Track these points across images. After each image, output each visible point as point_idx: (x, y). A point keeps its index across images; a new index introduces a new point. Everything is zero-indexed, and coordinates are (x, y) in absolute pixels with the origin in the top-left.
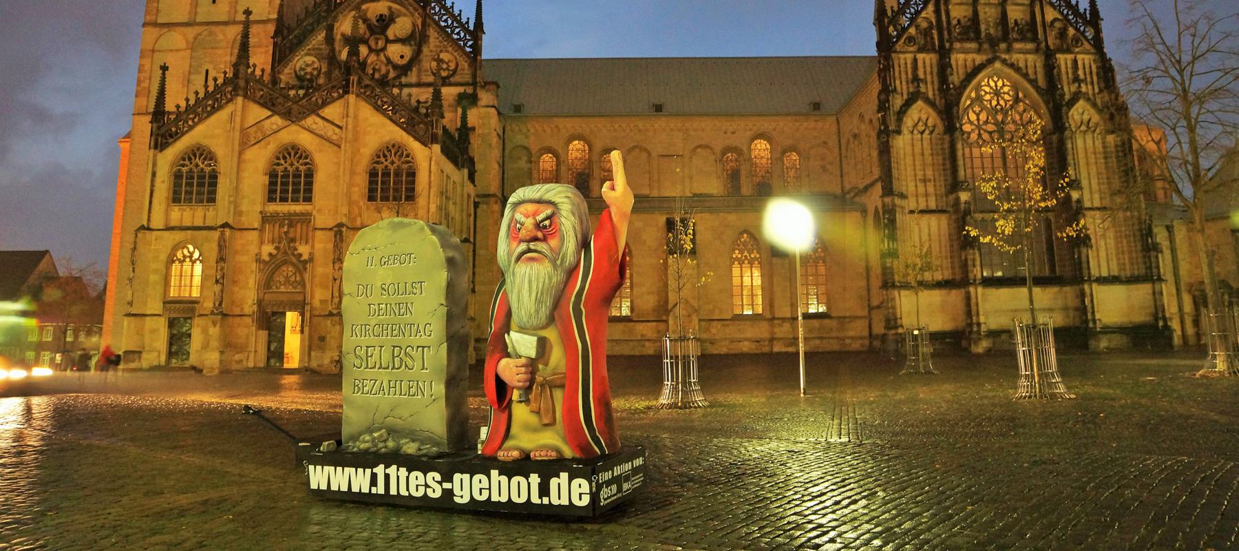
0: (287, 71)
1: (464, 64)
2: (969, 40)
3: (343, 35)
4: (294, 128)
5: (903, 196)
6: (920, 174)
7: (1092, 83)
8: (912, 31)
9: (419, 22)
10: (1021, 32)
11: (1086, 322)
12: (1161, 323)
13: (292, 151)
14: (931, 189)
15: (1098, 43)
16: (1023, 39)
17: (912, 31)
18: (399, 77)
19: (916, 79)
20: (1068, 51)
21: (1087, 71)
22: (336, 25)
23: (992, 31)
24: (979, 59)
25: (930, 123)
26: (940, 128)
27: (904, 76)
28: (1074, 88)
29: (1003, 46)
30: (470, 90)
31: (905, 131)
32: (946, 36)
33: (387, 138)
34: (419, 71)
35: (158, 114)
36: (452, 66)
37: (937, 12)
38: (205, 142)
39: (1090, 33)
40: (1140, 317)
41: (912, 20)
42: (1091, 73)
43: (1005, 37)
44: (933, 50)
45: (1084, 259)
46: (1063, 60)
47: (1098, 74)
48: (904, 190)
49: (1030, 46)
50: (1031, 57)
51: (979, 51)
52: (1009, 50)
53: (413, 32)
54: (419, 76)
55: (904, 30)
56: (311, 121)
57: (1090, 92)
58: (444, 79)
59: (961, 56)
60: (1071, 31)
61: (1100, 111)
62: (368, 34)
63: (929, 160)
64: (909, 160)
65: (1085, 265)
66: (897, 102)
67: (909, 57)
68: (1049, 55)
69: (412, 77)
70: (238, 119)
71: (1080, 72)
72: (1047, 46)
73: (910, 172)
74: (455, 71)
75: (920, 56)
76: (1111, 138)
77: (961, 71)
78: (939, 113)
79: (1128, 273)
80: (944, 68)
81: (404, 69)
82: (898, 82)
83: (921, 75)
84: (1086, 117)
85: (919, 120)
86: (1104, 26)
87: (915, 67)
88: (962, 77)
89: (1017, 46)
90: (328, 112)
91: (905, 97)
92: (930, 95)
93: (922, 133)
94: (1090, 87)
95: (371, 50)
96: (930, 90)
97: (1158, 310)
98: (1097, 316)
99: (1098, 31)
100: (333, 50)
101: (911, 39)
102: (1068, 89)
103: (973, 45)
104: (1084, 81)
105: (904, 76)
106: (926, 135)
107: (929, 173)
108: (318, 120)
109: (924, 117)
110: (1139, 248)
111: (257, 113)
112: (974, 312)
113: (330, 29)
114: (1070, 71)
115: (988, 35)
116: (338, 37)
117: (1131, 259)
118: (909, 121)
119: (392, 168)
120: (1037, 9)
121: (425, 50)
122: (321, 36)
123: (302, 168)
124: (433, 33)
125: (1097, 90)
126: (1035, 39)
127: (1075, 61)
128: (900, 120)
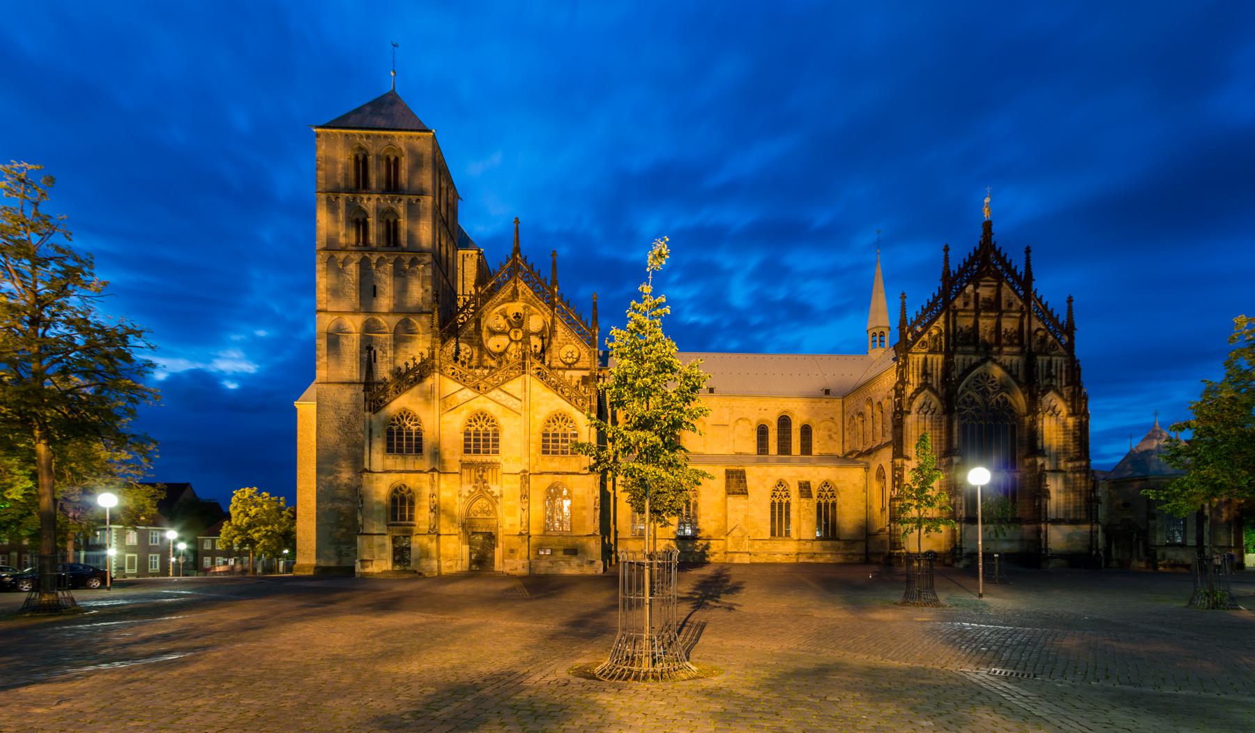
2: (968, 344)
4: (482, 398)
5: (908, 459)
8: (926, 337)
9: (549, 320)
10: (1010, 338)
11: (1040, 549)
13: (481, 416)
15: (1070, 347)
16: (1011, 344)
20: (1046, 354)
23: (987, 338)
24: (975, 359)
28: (1046, 382)
29: (995, 349)
31: (913, 411)
33: (555, 408)
36: (576, 355)
37: (947, 322)
39: (1065, 339)
40: (1079, 547)
43: (998, 342)
44: (940, 352)
46: (1041, 360)
49: (1016, 349)
50: (1015, 358)
51: (976, 353)
52: (1000, 352)
53: (544, 328)
55: (919, 335)
56: (495, 394)
58: (570, 365)
59: (961, 357)
60: (1050, 338)
62: (508, 328)
66: (910, 390)
67: (922, 357)
71: (1053, 371)
72: (1030, 349)
74: (578, 360)
75: (930, 356)
77: (960, 368)
78: (940, 399)
79: (1072, 517)
86: (1076, 334)
88: (960, 372)
89: (1006, 349)
90: (508, 387)
95: (511, 340)
99: (1072, 338)
101: (923, 343)
103: (971, 349)
104: (1055, 377)
108: (500, 393)
115: (984, 341)
116: (485, 329)
119: (481, 430)
121: (553, 341)
123: (414, 428)
124: (560, 328)
127: (1050, 362)
128: (910, 404)
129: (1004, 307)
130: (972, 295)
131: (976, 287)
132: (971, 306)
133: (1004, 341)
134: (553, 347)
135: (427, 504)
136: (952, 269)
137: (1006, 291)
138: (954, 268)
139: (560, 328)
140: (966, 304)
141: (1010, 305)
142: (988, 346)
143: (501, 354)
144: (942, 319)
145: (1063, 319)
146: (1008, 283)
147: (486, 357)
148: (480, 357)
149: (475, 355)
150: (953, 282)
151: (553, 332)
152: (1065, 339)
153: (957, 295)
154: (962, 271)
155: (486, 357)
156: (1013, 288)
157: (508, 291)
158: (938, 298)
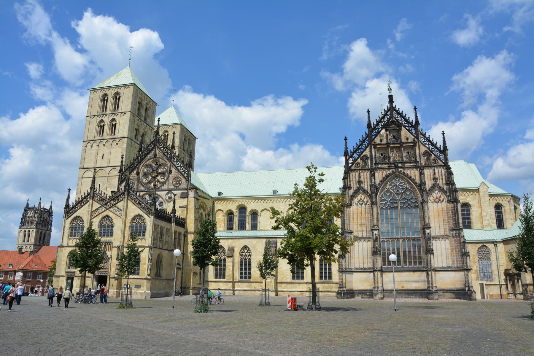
1: (184, 181)
6: (360, 222)
7: (442, 179)
8: (359, 160)
12: (467, 289)
14: (364, 228)
17: (359, 160)
18: (161, 186)
19: (360, 182)
21: (440, 173)
22: (140, 167)
25: (366, 200)
26: (369, 203)
27: (354, 180)
30: (186, 191)
32: (374, 162)
34: (168, 184)
35: (67, 206)
38: (80, 215)
41: (359, 156)
42: (442, 174)
45: (429, 259)
47: (445, 175)
48: (352, 229)
51: (389, 168)
54: (168, 186)
55: (356, 160)
57: (441, 183)
58: (177, 187)
60: (433, 156)
61: (445, 192)
63: (364, 215)
64: (355, 216)
65: (429, 262)
66: (351, 192)
68: (421, 169)
69: (165, 187)
70: (90, 207)
72: (421, 164)
73: (355, 221)
74: (180, 184)
76: (450, 206)
78: (370, 196)
80: (373, 176)
81: (163, 184)
82: (352, 183)
83: (362, 179)
84: (439, 195)
85: (361, 199)
86: (449, 152)
87: (360, 177)
88: (381, 179)
89: (406, 165)
91: (355, 189)
92: (366, 188)
93: (361, 204)
94: (441, 181)
95: (152, 177)
96: (366, 186)
97: (467, 284)
98: (434, 285)
100: (139, 177)
102: (429, 183)
103: (386, 166)
105: (354, 180)
106: (363, 206)
107: (364, 222)
109: (363, 198)
110: (460, 254)
111: (96, 205)
112: (376, 282)
113: (138, 168)
114: (432, 174)
117: (456, 259)
118: (356, 200)
120: (417, 148)
121: (170, 175)
124: (173, 169)
125: (444, 182)
126: (416, 162)
129: (403, 140)
130: (385, 135)
131: (386, 130)
132: (384, 141)
133: (405, 159)
134: (170, 178)
135: (63, 273)
136: (372, 123)
137: (404, 132)
138: (373, 121)
139: (173, 169)
140: (381, 141)
141: (407, 139)
142: (396, 164)
143: (147, 184)
144: (368, 150)
145: (440, 144)
146: (405, 127)
147: (140, 185)
148: (138, 185)
149: (136, 185)
150: (374, 129)
151: (170, 172)
152: (442, 156)
153: (376, 135)
154: (379, 122)
155: (140, 185)
156: (408, 130)
157: (152, 153)
158: (366, 139)
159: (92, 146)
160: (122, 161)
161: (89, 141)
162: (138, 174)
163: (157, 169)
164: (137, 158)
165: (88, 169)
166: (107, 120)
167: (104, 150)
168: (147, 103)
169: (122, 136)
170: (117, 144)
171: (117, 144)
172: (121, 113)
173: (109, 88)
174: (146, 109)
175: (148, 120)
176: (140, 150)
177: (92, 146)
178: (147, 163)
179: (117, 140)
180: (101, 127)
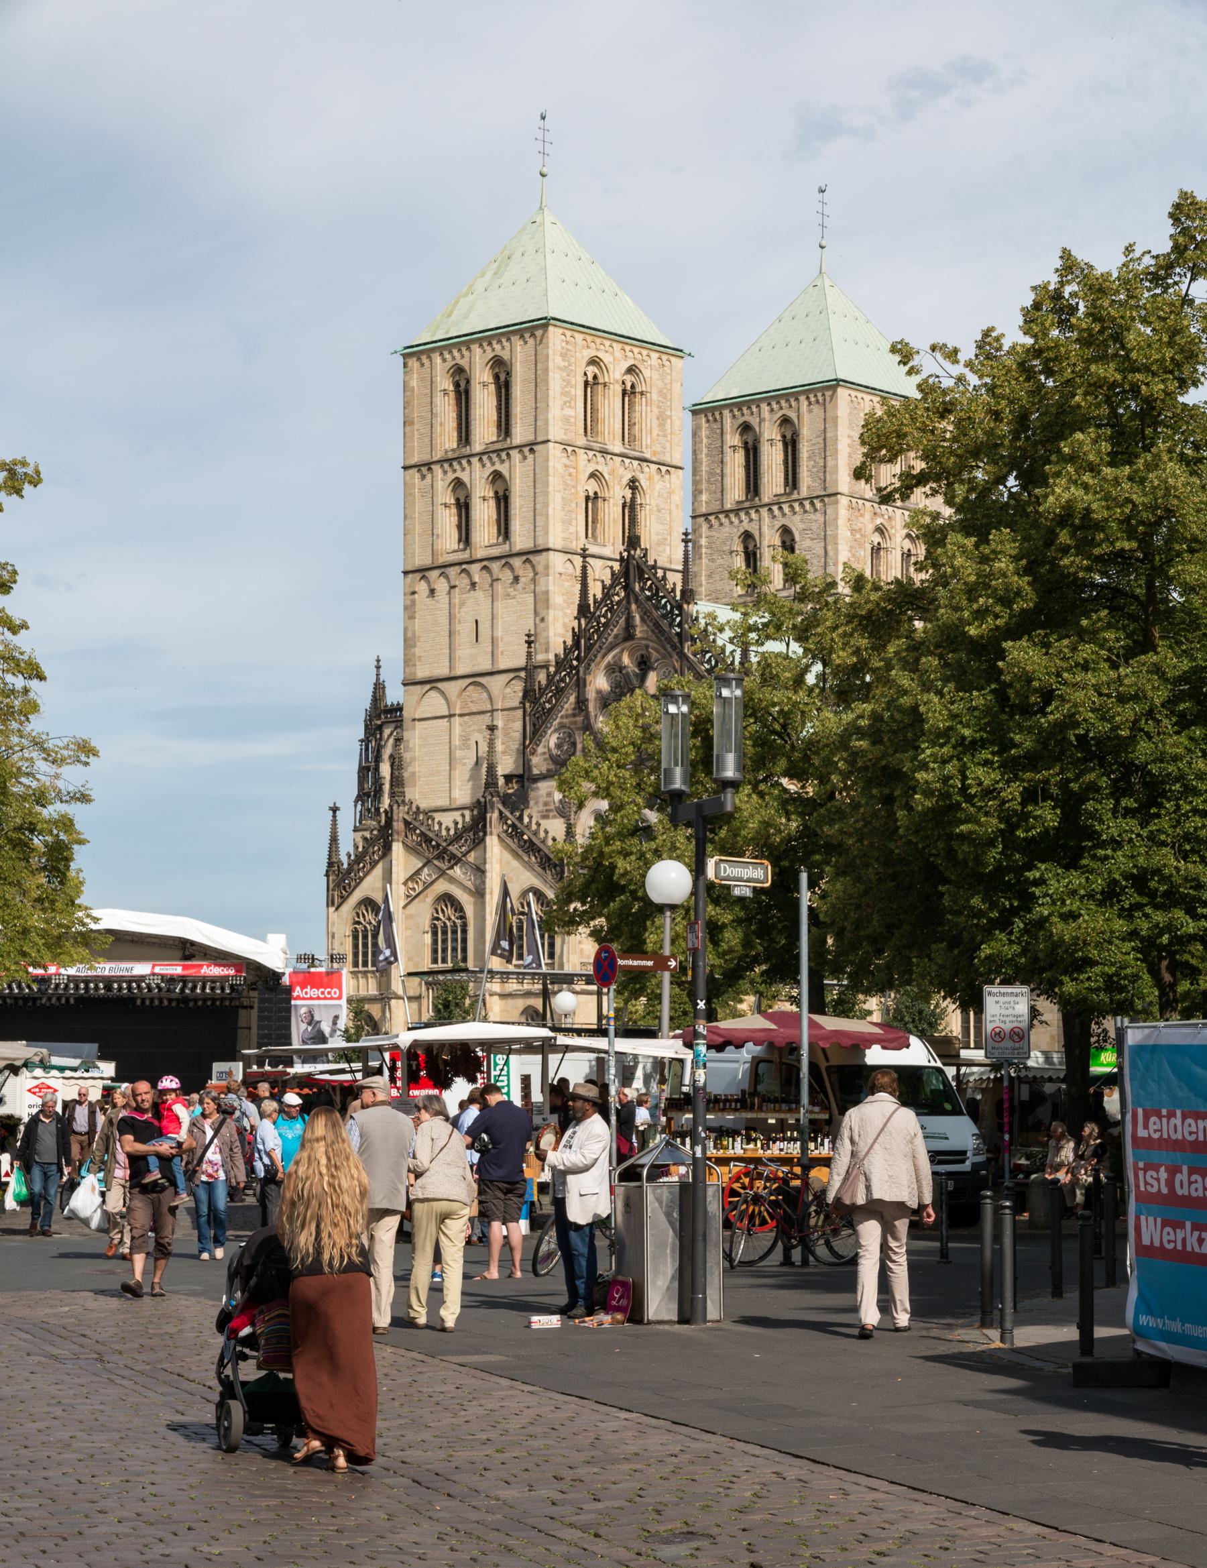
0: (540, 750)
3: (599, 692)
22: (589, 678)
100: (587, 716)
113: (580, 685)
122: (572, 699)
159: (432, 592)
160: (529, 655)
161: (422, 571)
162: (581, 704)
163: (643, 678)
164: (576, 644)
165: (432, 682)
166: (478, 479)
167: (475, 605)
168: (631, 370)
169: (529, 545)
170: (516, 579)
171: (516, 579)
172: (520, 447)
173: (466, 341)
174: (629, 393)
175: (646, 440)
176: (583, 609)
177: (432, 592)
178: (610, 657)
179: (517, 562)
180: (463, 507)
